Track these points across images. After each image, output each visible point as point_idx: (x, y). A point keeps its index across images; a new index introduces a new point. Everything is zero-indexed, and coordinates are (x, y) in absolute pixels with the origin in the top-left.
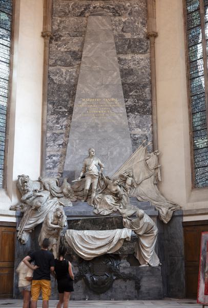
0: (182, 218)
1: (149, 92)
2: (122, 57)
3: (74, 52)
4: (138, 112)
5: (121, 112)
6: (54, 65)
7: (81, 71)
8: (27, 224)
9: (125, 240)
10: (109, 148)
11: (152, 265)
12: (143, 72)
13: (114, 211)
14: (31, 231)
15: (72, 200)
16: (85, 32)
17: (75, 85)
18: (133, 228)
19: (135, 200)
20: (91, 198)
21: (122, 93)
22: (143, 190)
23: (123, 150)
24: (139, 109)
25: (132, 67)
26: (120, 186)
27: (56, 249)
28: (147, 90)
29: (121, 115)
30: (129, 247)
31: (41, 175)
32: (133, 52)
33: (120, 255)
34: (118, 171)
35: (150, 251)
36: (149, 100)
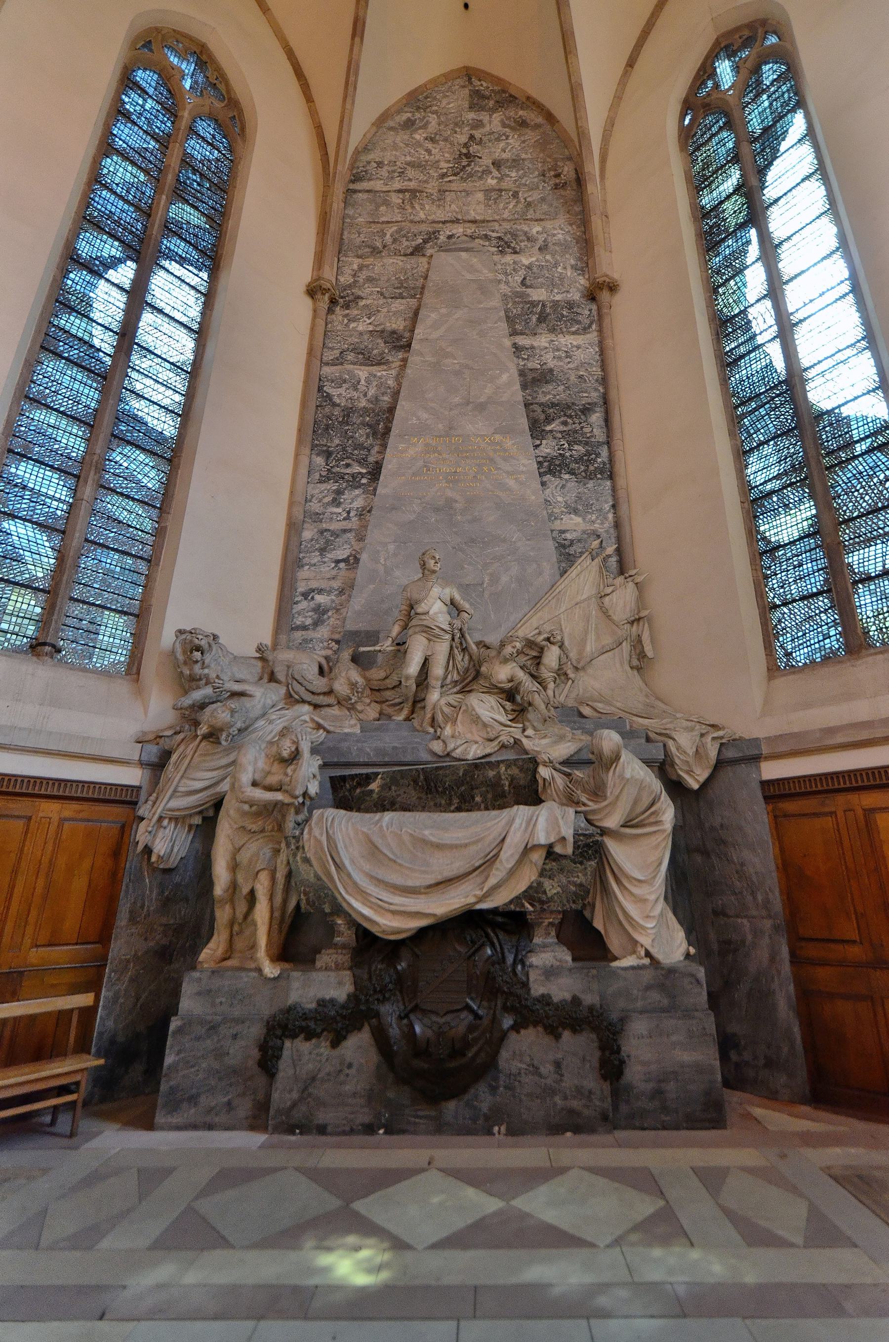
1: (603, 424)
2: (522, 341)
3: (394, 332)
4: (572, 472)
5: (522, 468)
6: (338, 361)
7: (408, 371)
9: (550, 853)
12: (581, 377)
13: (503, 746)
15: (361, 716)
16: (423, 288)
17: (391, 410)
20: (424, 707)
21: (524, 423)
24: (573, 466)
25: (551, 364)
28: (596, 418)
29: (523, 477)
32: (552, 330)
36: (600, 444)
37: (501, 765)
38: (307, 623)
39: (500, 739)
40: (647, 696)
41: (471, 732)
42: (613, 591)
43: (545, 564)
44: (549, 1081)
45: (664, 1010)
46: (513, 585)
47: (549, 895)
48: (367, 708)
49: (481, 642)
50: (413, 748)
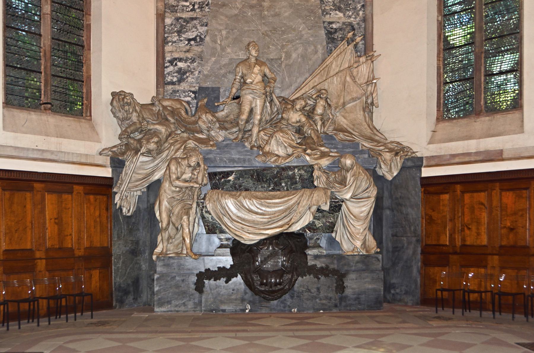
10: (283, 47)
23: (310, 50)
38: (174, 80)
43: (319, 46)
44: (315, 294)
45: (364, 270)
46: (299, 60)
47: (317, 226)
50: (249, 159)
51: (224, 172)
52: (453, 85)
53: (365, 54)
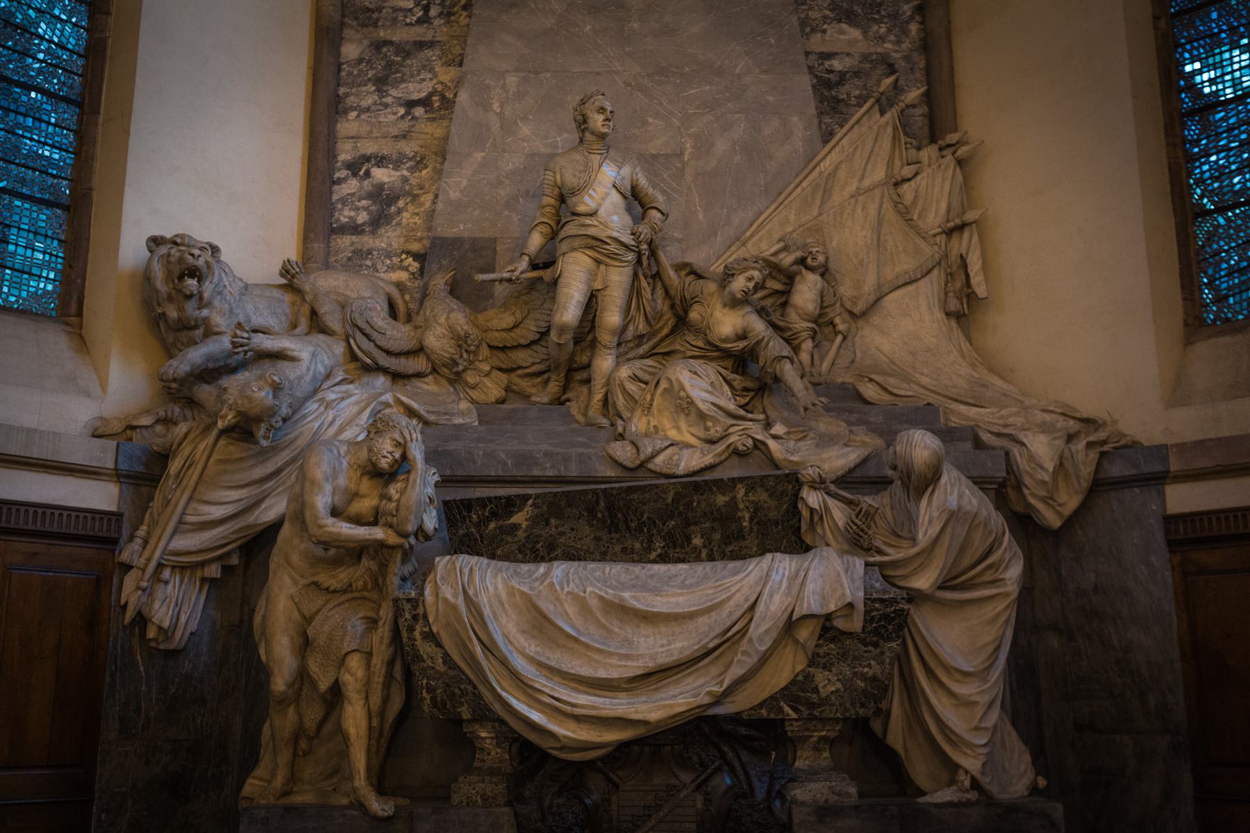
0: (1162, 495)
8: (181, 527)
9: (826, 626)
11: (994, 789)
13: (736, 453)
14: (214, 571)
15: (474, 394)
18: (868, 550)
19: (845, 400)
20: (588, 381)
22: (886, 347)
26: (761, 312)
27: (368, 682)
30: (847, 671)
31: (306, 257)
33: (792, 729)
34: (738, 239)
35: (986, 699)
37: (739, 486)
38: (360, 220)
39: (732, 439)
40: (973, 365)
41: (678, 428)
42: (916, 174)
48: (485, 380)
49: (685, 265)
50: (581, 455)
51: (499, 498)
52: (1228, 219)
53: (933, 140)
